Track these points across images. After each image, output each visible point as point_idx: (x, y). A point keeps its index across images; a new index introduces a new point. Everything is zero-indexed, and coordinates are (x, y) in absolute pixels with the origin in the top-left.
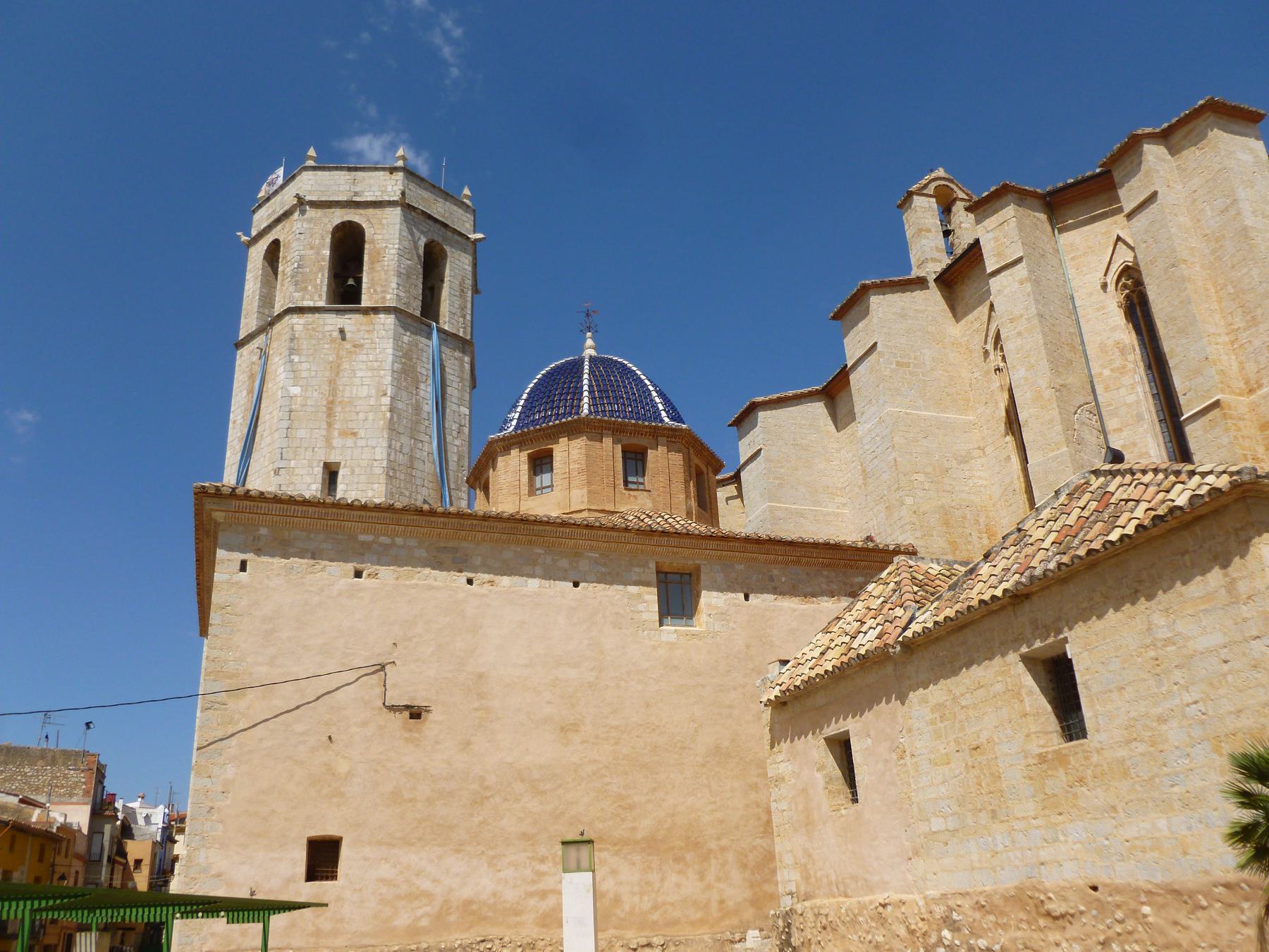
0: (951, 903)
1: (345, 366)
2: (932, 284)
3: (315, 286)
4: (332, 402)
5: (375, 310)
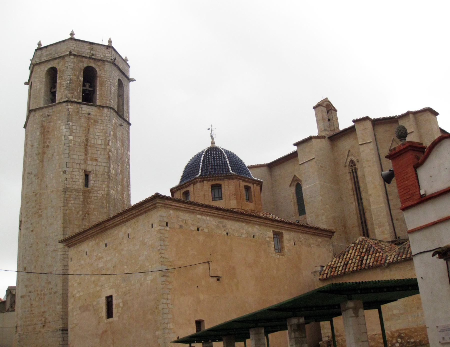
0: (401, 332)
1: (91, 130)
2: (327, 138)
3: (77, 93)
4: (87, 145)
5: (103, 107)
